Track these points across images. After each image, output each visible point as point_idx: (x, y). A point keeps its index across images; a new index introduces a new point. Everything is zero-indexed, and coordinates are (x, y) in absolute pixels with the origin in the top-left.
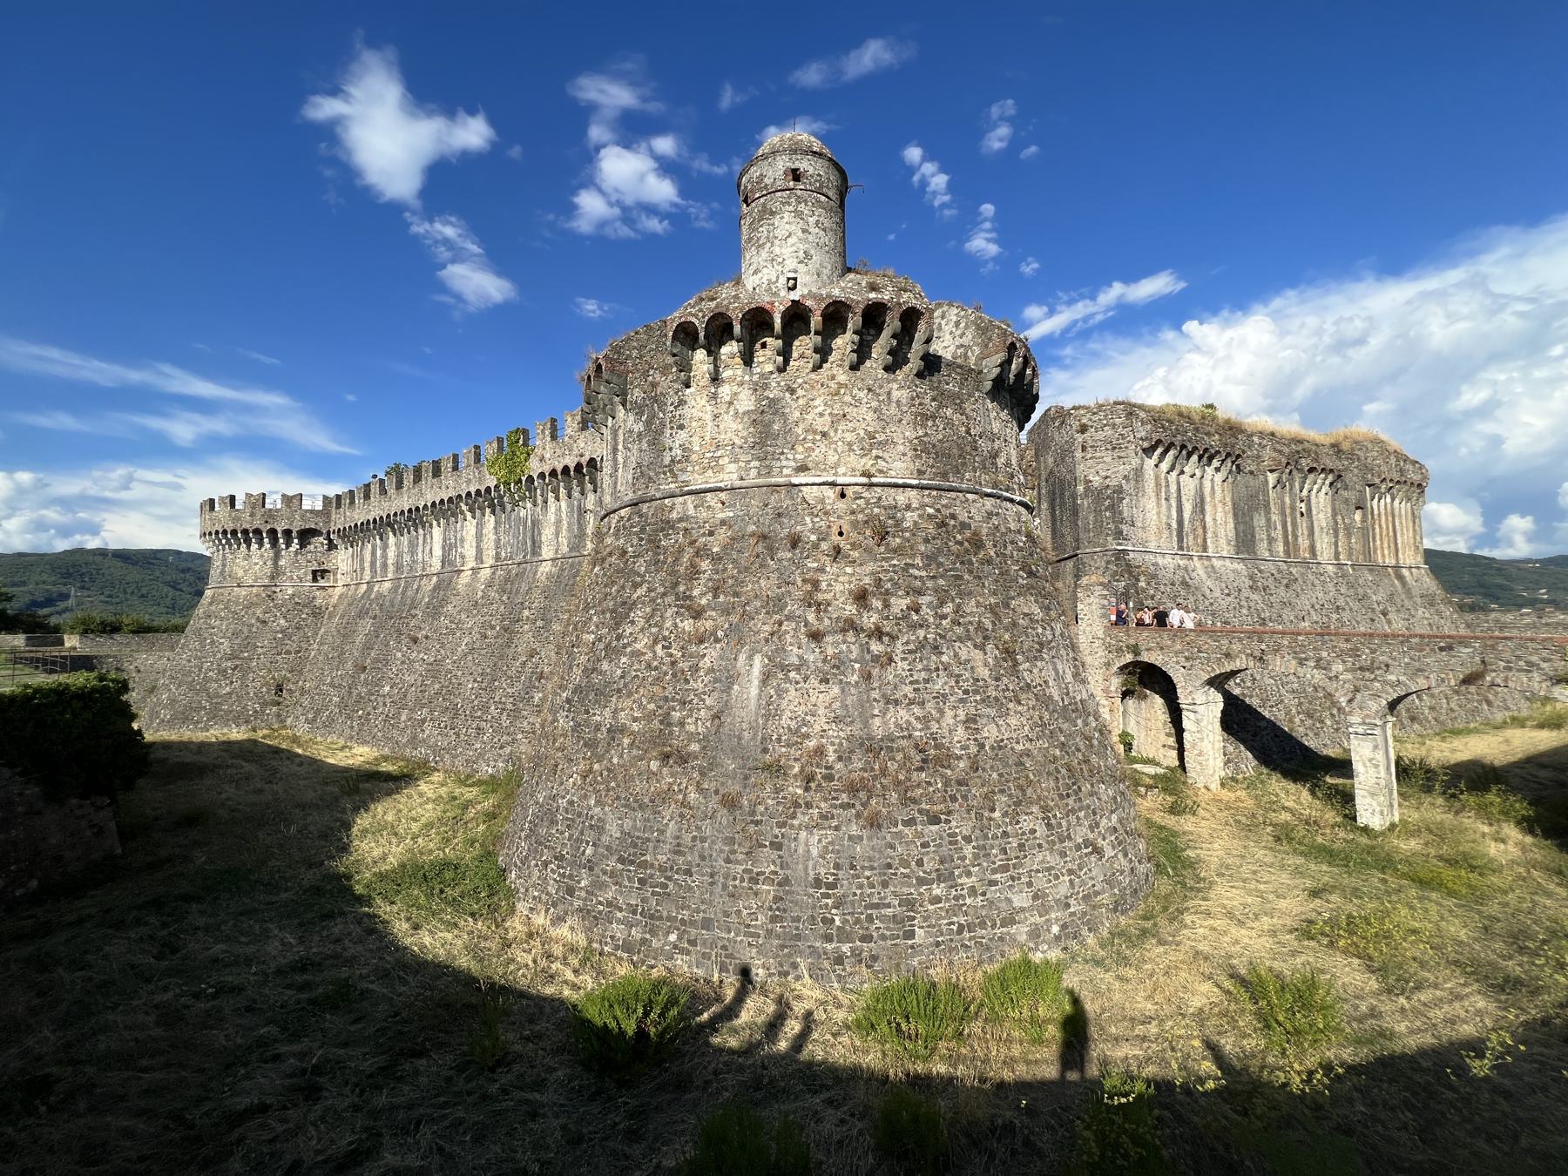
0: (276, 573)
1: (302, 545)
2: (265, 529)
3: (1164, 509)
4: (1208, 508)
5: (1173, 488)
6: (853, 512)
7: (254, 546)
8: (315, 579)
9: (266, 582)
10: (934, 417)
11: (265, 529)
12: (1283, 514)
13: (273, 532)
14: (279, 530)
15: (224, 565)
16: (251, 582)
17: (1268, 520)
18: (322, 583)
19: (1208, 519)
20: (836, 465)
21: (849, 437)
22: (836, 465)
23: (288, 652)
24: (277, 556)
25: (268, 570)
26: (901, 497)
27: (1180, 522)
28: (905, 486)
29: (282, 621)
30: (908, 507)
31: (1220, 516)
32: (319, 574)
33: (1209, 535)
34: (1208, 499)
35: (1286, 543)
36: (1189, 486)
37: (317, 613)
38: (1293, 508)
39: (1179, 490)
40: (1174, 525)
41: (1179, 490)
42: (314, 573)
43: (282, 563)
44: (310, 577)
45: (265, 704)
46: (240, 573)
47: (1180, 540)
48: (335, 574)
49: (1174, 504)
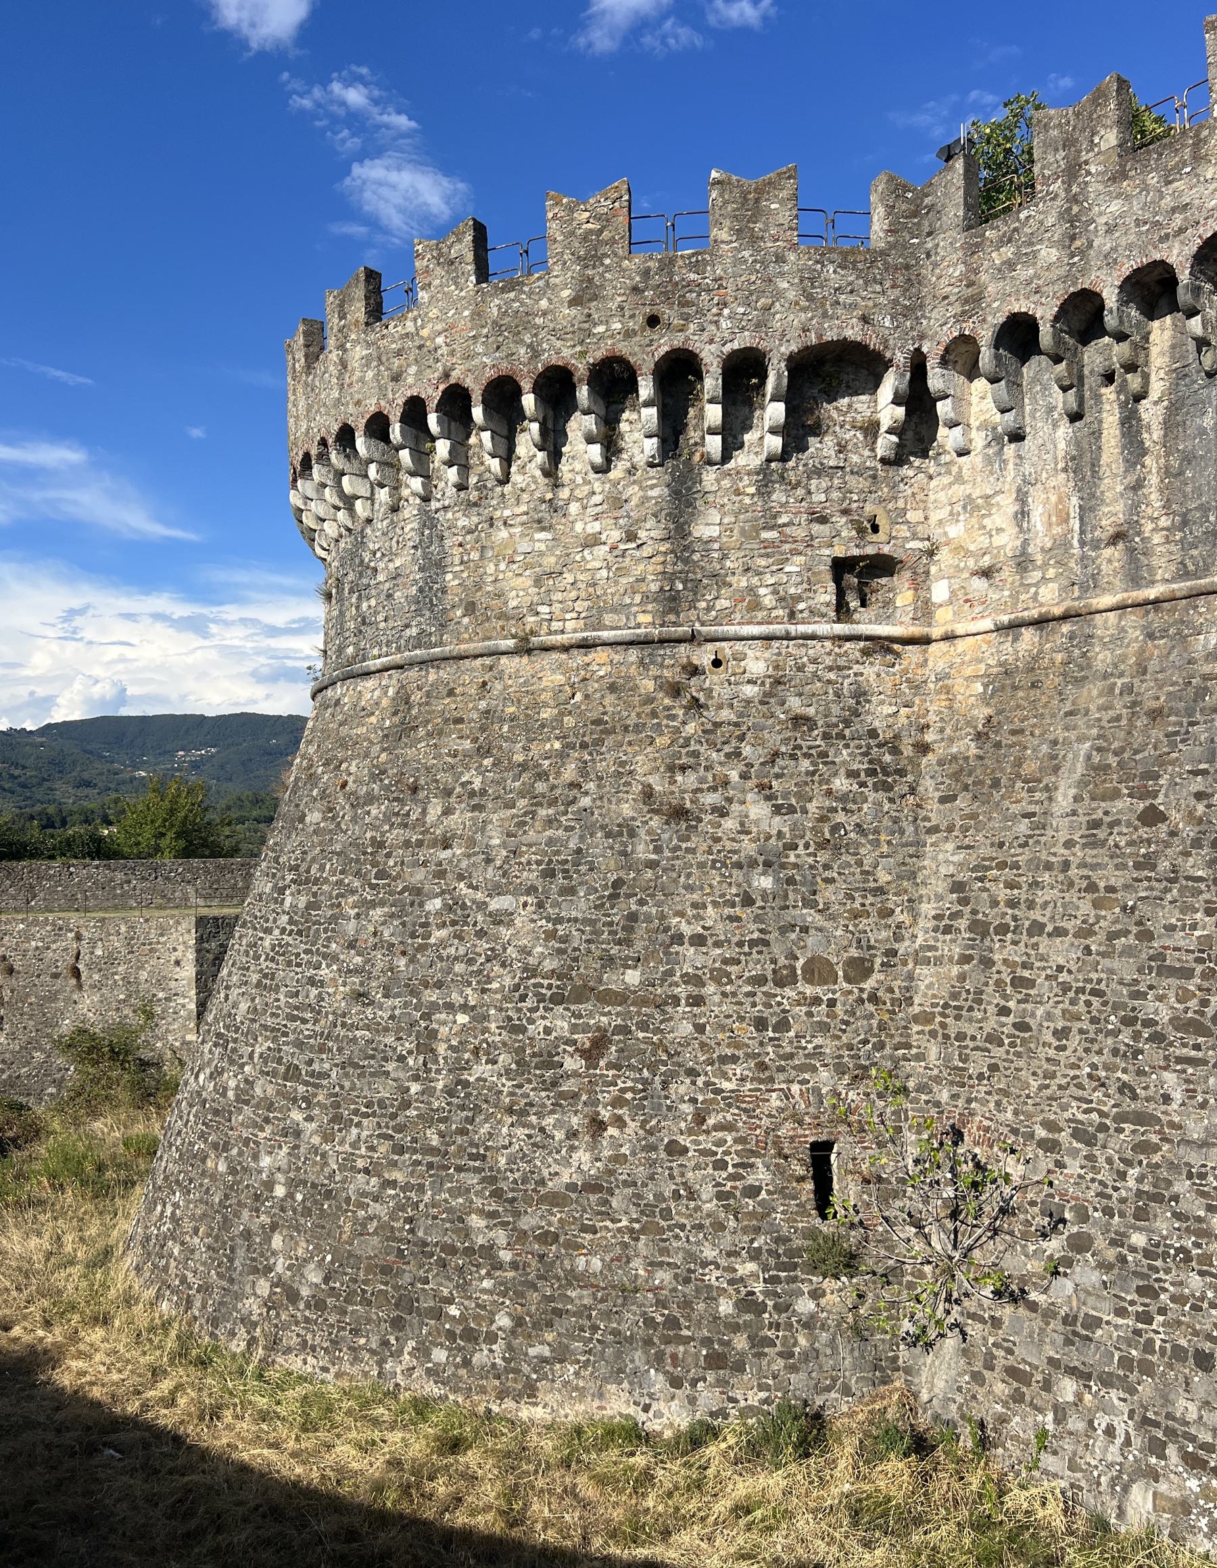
0: (684, 580)
1: (797, 432)
2: (645, 354)
7: (581, 450)
8: (842, 611)
9: (645, 622)
11: (645, 354)
13: (679, 372)
14: (711, 358)
15: (434, 566)
16: (573, 631)
18: (868, 624)
23: (818, 971)
24: (683, 501)
25: (647, 566)
29: (758, 810)
32: (859, 575)
37: (888, 765)
42: (840, 567)
43: (707, 527)
44: (826, 595)
45: (784, 1262)
46: (518, 590)
48: (921, 581)
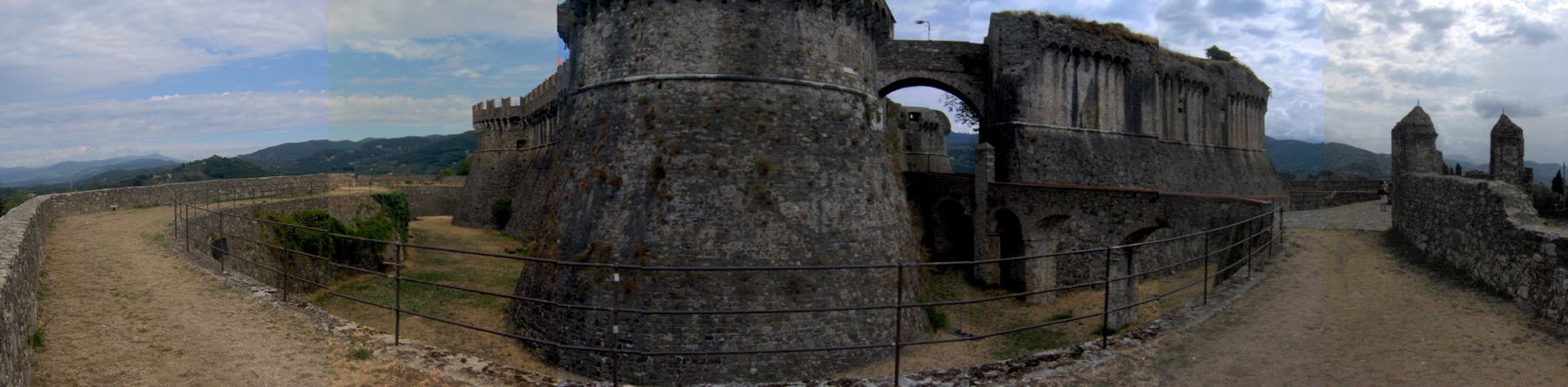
3: (1060, 96)
4: (1101, 96)
5: (1070, 80)
6: (664, 98)
10: (737, 31)
12: (1164, 109)
17: (1154, 108)
19: (1101, 103)
20: (659, 67)
21: (669, 48)
22: (659, 67)
26: (702, 87)
27: (1075, 106)
28: (705, 79)
30: (705, 94)
31: (1111, 103)
33: (1101, 115)
34: (1102, 89)
35: (1165, 130)
36: (1085, 78)
38: (1172, 104)
39: (1076, 82)
40: (1069, 107)
41: (1076, 82)
47: (1074, 118)
49: (1070, 91)
